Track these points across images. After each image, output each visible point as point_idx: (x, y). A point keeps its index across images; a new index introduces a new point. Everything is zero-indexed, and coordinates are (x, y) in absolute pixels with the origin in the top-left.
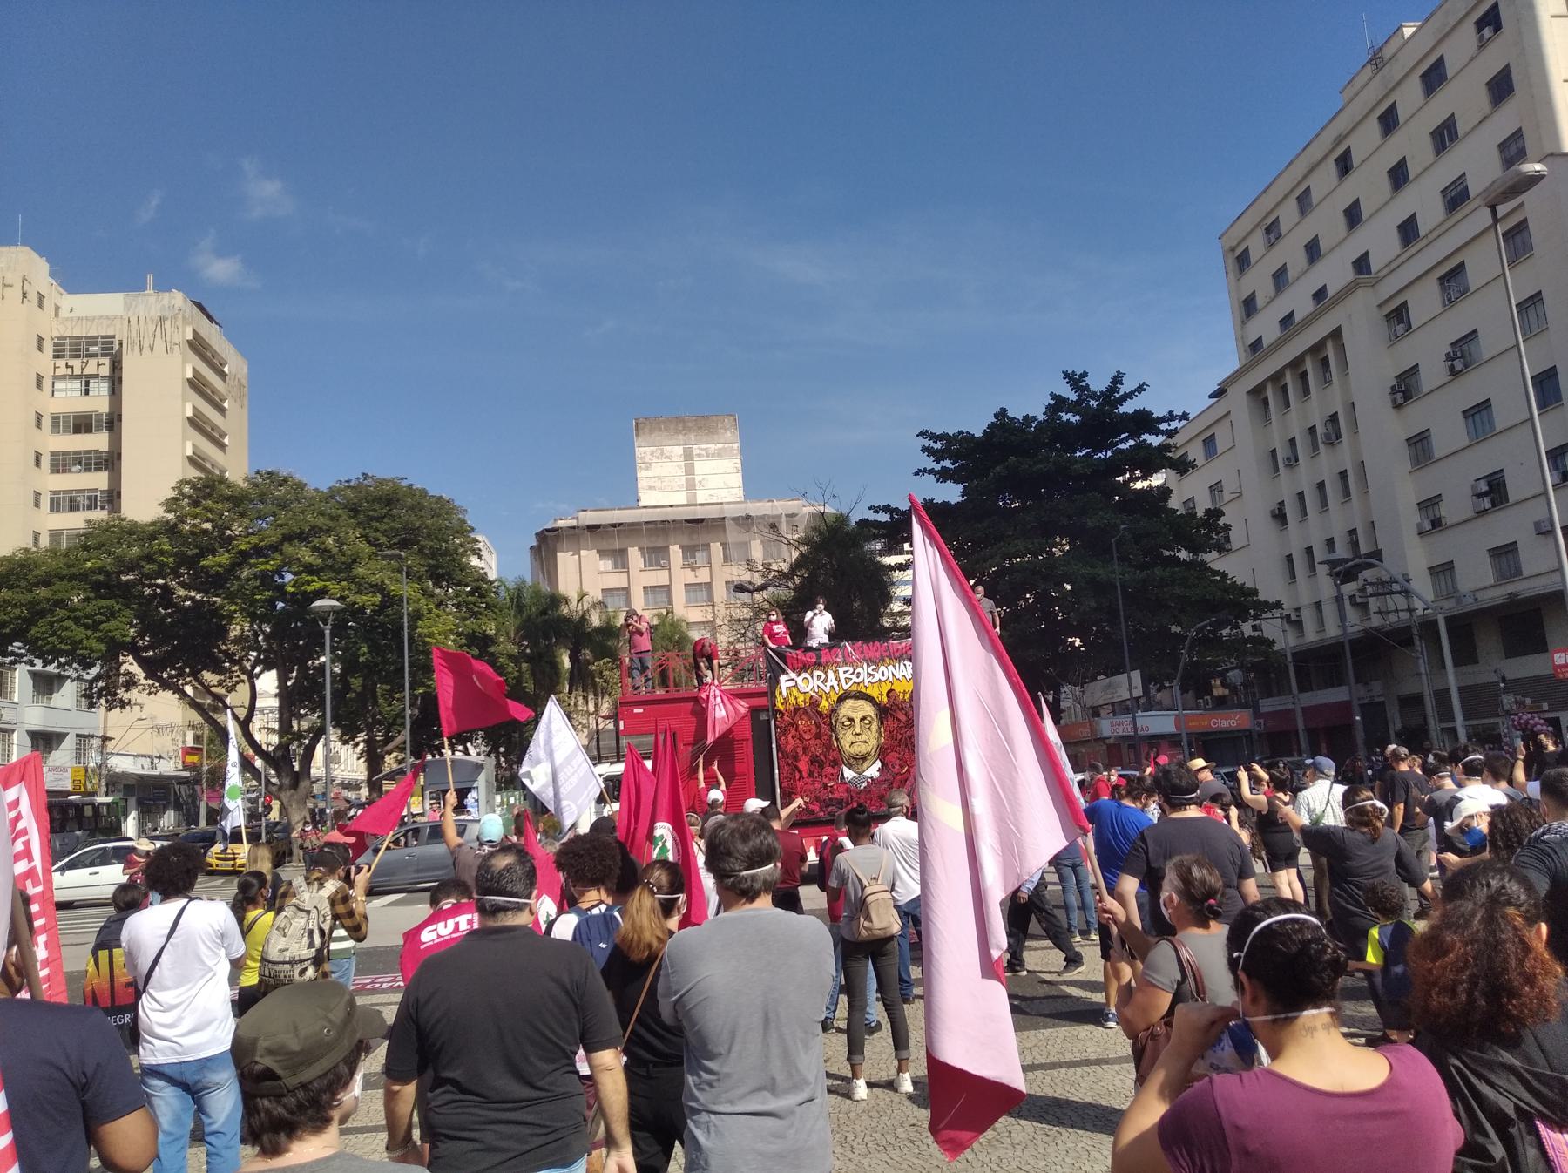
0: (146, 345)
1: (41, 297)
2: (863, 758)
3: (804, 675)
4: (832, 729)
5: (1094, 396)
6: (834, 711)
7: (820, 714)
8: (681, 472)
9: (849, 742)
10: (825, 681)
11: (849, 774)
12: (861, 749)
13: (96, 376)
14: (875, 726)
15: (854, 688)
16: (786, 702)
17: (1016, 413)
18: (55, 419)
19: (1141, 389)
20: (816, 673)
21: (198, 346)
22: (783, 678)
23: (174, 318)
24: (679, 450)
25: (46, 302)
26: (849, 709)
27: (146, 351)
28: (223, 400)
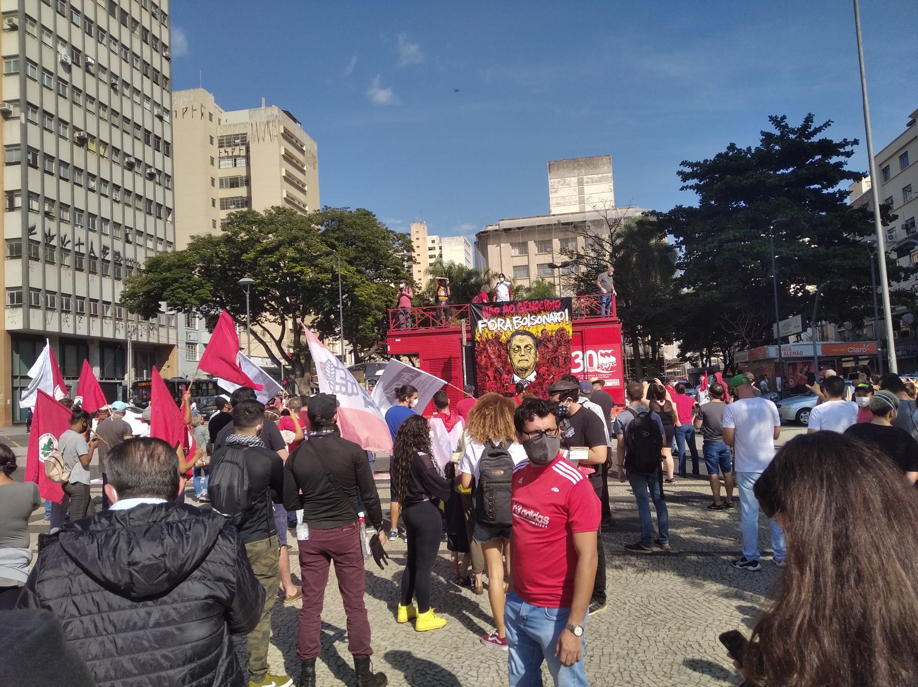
1: (211, 115)
2: (526, 370)
3: (492, 321)
4: (508, 352)
5: (793, 131)
6: (509, 341)
7: (501, 343)
8: (576, 193)
9: (517, 360)
10: (504, 325)
11: (517, 379)
12: (524, 364)
13: (239, 156)
14: (533, 351)
15: (522, 328)
16: (481, 336)
17: (742, 145)
18: (221, 180)
19: (827, 124)
20: (499, 320)
21: (287, 136)
22: (480, 322)
23: (274, 121)
24: (575, 180)
25: (213, 117)
26: (517, 341)
27: (261, 140)
28: (303, 166)
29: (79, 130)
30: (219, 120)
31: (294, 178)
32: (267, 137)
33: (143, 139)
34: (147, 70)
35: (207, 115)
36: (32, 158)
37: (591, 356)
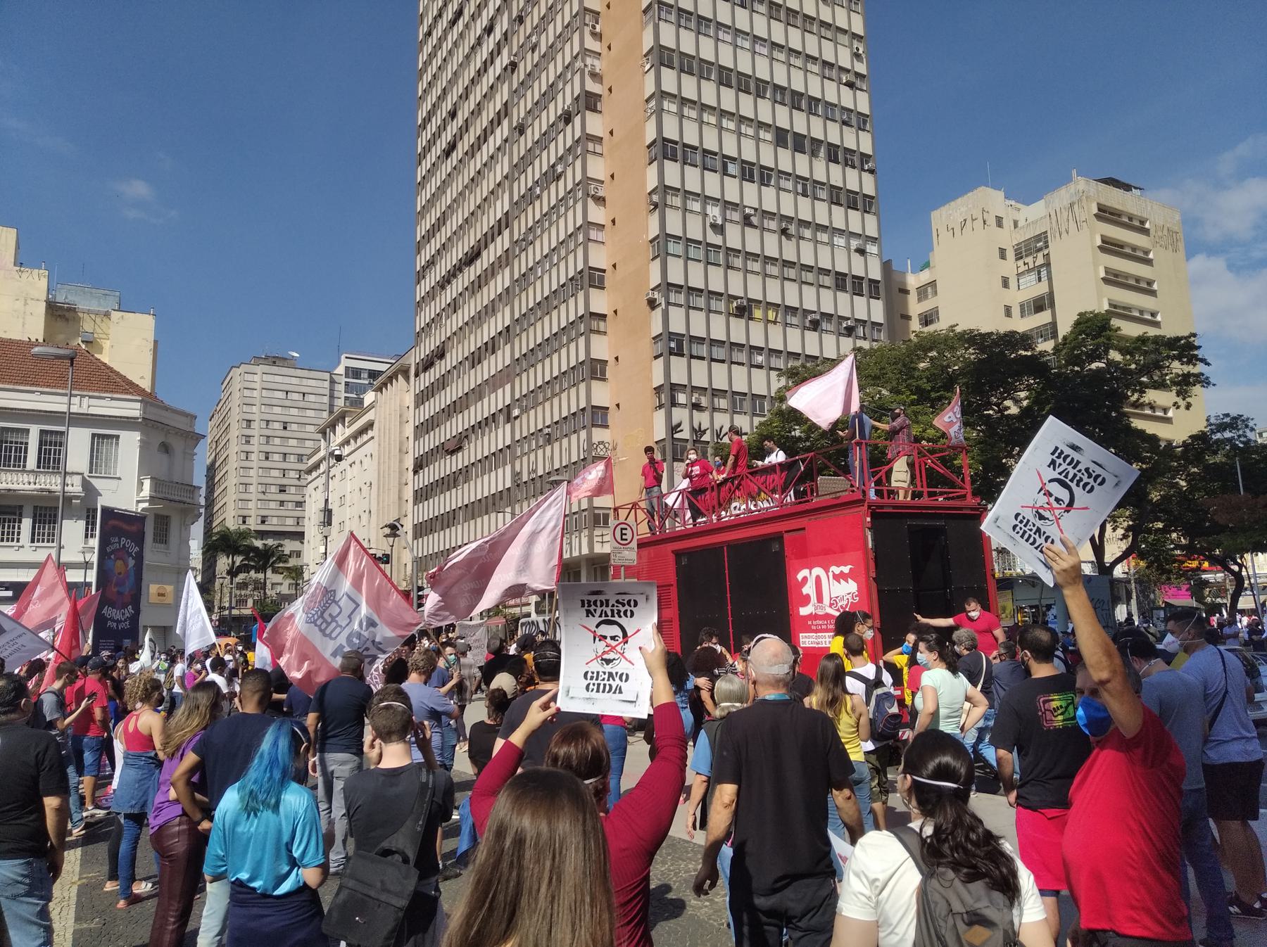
0: (1063, 230)
21: (1106, 214)
23: (1080, 200)
27: (1064, 234)
29: (736, 298)
31: (1127, 276)
32: (1072, 225)
33: (833, 286)
34: (838, 196)
36: (675, 345)
37: (818, 579)
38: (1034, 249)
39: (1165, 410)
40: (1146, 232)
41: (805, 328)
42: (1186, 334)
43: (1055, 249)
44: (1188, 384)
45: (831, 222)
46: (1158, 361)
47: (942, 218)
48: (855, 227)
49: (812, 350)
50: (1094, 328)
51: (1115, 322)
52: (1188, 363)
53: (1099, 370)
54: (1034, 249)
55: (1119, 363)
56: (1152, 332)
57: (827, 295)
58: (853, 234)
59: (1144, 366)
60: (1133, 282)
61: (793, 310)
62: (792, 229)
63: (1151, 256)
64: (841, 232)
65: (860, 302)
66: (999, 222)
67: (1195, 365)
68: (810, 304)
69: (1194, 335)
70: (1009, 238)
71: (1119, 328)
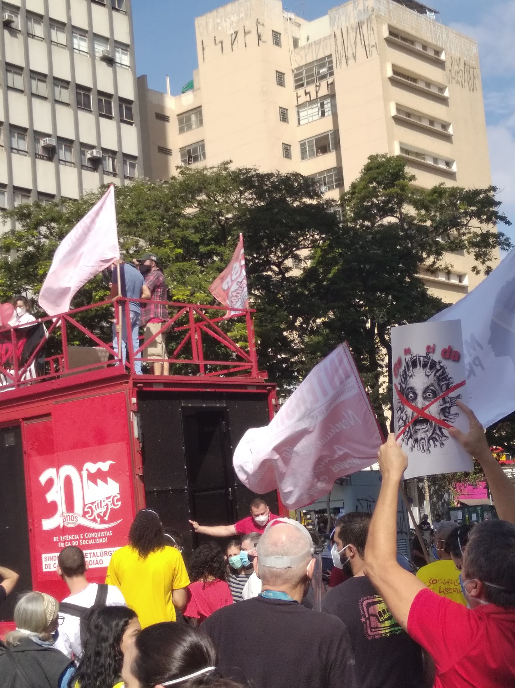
0: (350, 55)
21: (398, 39)
23: (369, 20)
27: (351, 61)
28: (442, 89)
30: (296, 42)
31: (420, 116)
32: (361, 51)
33: (73, 102)
35: (268, 37)
38: (316, 74)
39: (460, 277)
40: (440, 64)
41: (36, 156)
42: (485, 187)
43: (341, 77)
44: (488, 245)
45: (69, 18)
46: (456, 218)
47: (208, 27)
48: (101, 27)
49: (47, 185)
50: (386, 174)
51: (409, 170)
52: (488, 220)
53: (391, 226)
54: (316, 74)
55: (413, 218)
56: (449, 184)
57: (65, 115)
58: (98, 37)
59: (440, 222)
60: (426, 123)
61: (21, 131)
62: (18, 22)
63: (446, 94)
64: (82, 32)
65: (109, 127)
66: (277, 38)
67: (494, 223)
68: (42, 125)
69: (494, 189)
70: (288, 60)
71: (413, 178)
